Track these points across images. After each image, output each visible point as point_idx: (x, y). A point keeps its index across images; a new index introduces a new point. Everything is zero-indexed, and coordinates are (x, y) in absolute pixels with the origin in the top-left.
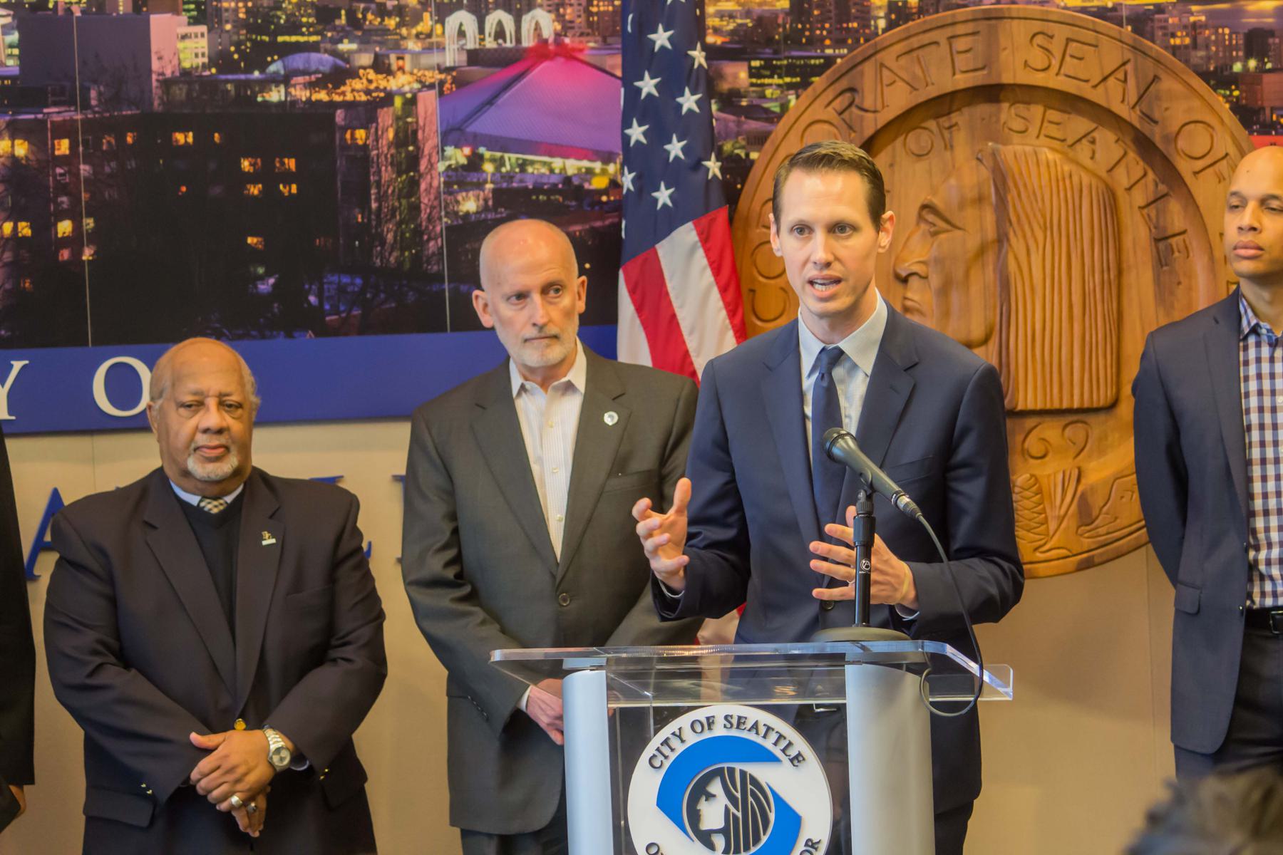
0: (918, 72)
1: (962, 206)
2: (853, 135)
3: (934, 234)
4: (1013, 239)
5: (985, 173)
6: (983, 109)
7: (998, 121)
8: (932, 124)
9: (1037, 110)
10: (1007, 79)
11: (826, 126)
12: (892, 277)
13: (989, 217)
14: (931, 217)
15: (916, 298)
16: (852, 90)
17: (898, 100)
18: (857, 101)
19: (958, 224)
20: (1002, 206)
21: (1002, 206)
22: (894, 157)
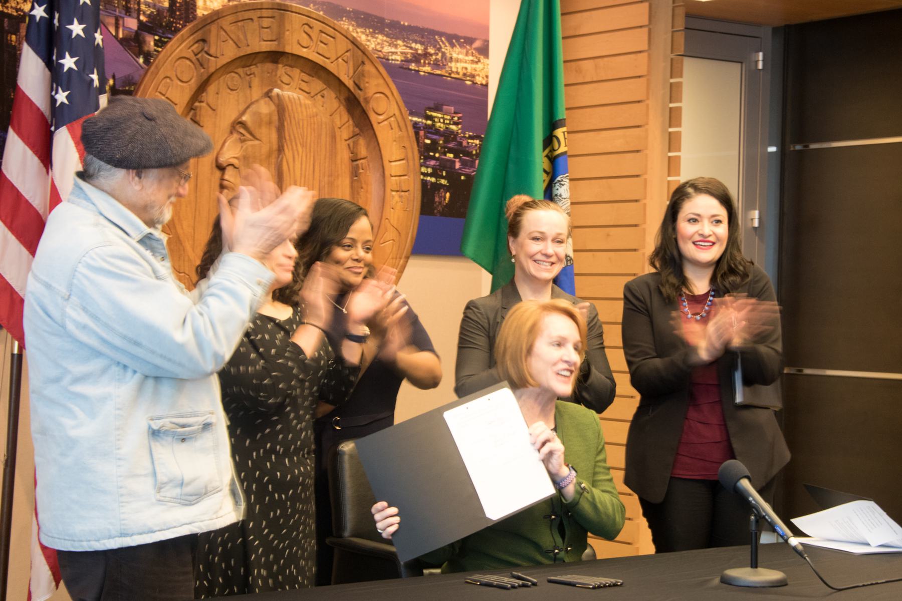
0: (242, 37)
1: (260, 126)
2: (202, 70)
3: (243, 141)
4: (286, 150)
5: (273, 107)
6: (269, 66)
7: (276, 75)
8: (240, 71)
9: (296, 72)
10: (288, 49)
11: (188, 62)
12: (214, 165)
13: (274, 136)
14: (242, 131)
15: (232, 180)
16: (204, 41)
17: (229, 52)
18: (206, 49)
19: (258, 136)
20: (280, 130)
21: (280, 130)
22: (219, 89)
